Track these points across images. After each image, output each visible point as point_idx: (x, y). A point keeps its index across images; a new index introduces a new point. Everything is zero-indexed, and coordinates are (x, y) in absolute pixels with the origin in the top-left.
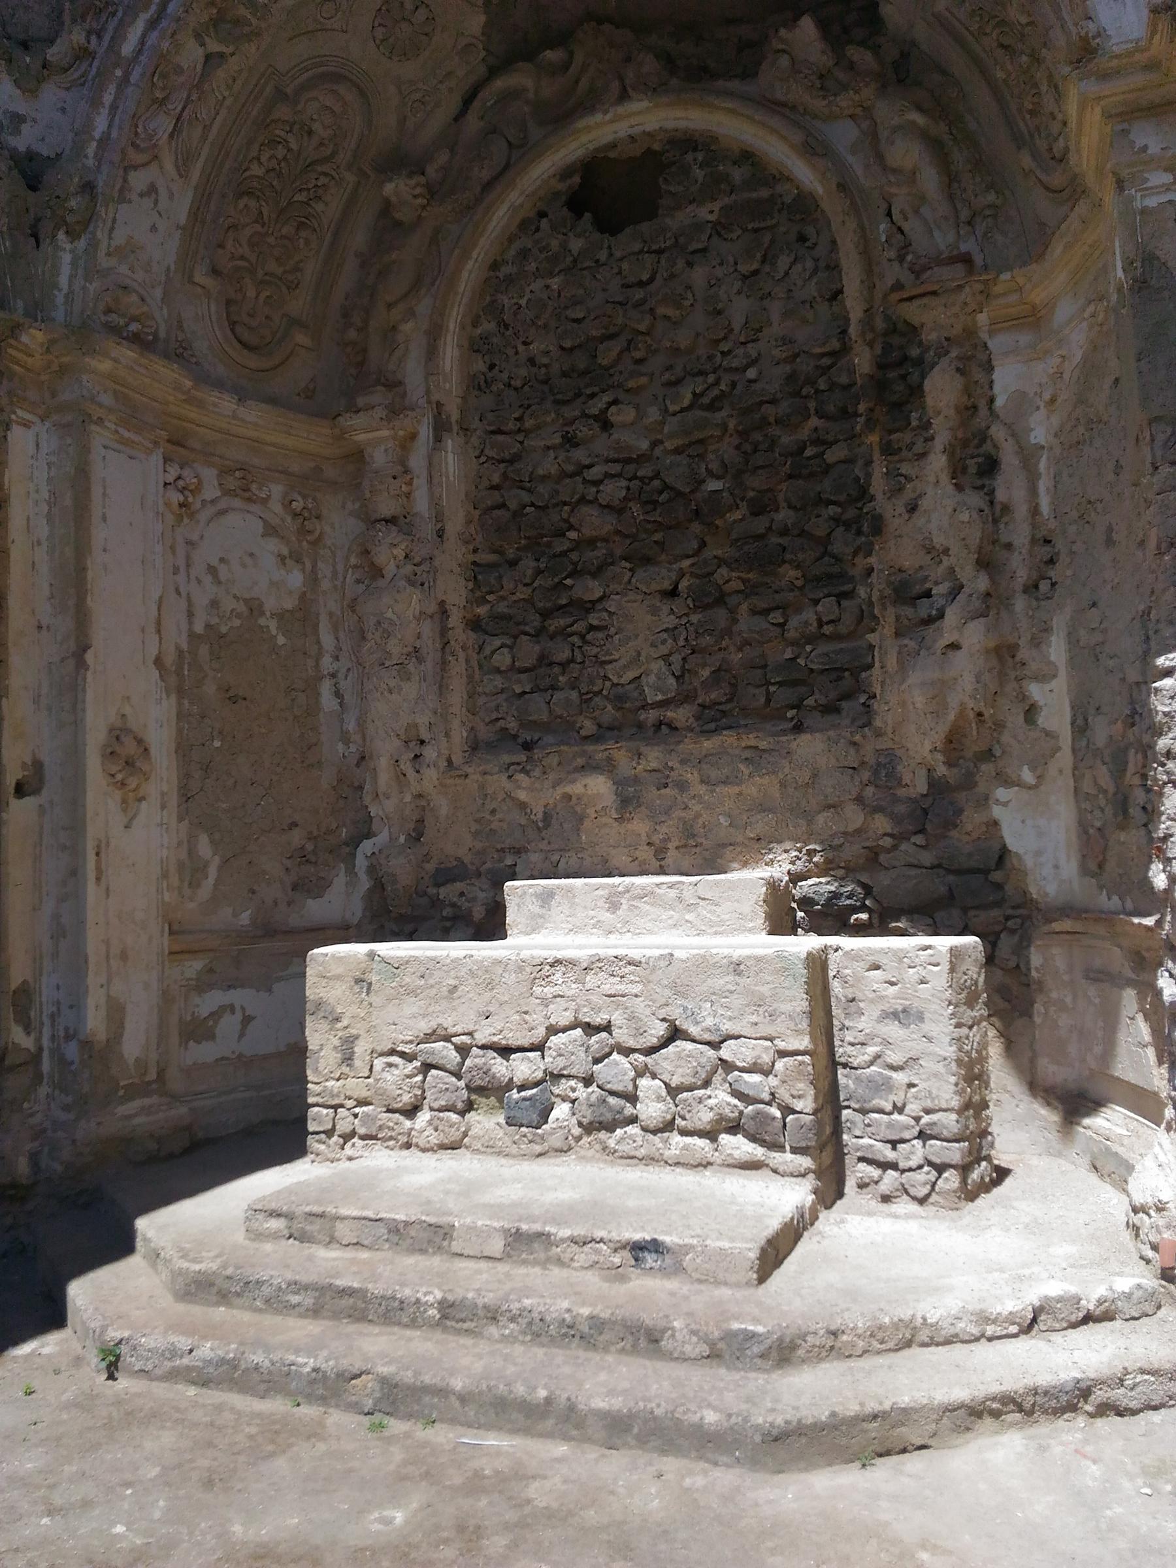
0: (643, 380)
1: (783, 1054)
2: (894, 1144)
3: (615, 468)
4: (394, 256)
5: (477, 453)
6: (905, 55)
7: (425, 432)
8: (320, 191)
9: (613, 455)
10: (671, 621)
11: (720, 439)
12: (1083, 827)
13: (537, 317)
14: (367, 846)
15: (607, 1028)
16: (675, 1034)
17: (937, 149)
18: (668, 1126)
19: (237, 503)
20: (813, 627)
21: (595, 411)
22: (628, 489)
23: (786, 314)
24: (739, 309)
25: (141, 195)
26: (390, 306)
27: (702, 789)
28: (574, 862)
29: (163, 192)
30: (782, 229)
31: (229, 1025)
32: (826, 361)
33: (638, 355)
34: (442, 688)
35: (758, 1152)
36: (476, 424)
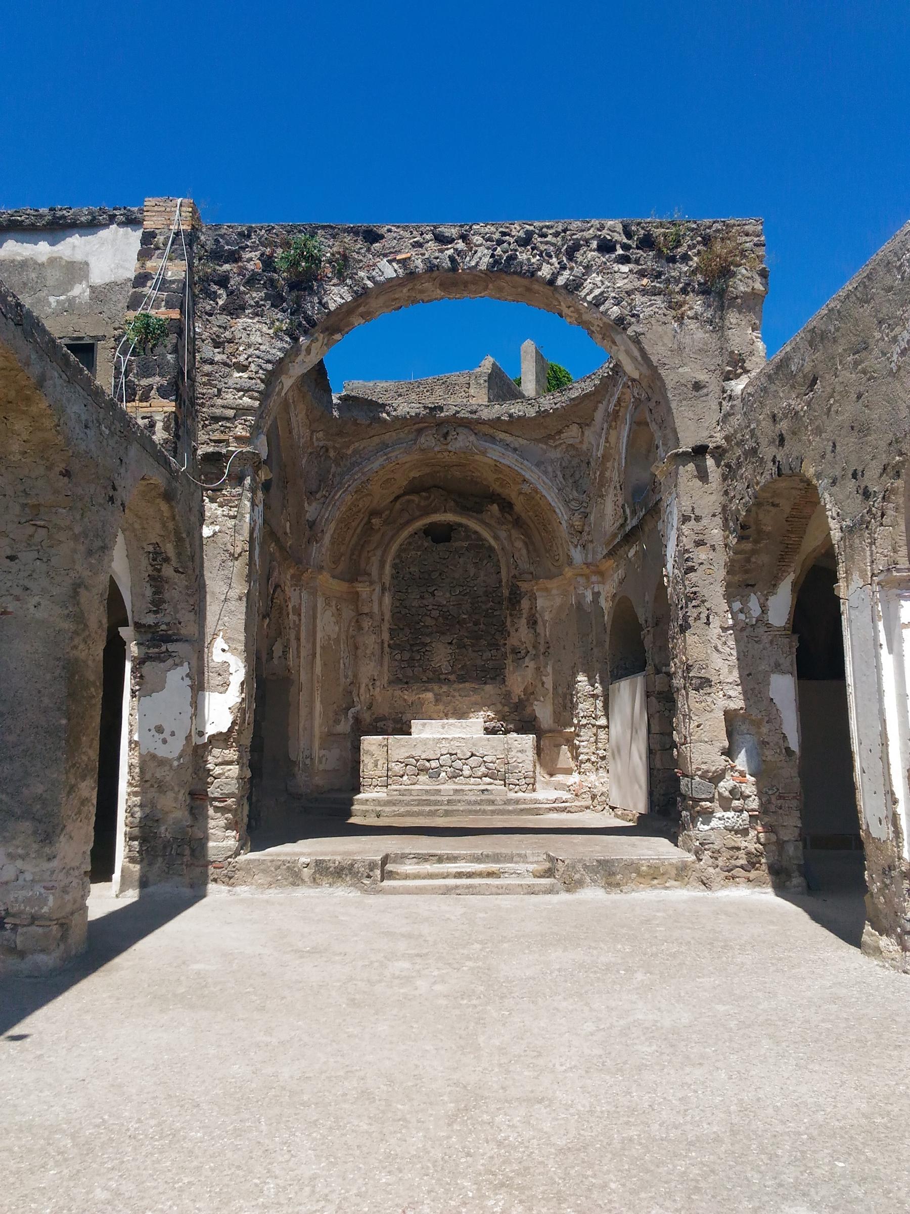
3: (436, 607)
7: (378, 588)
10: (451, 651)
12: (554, 712)
14: (353, 710)
15: (456, 754)
16: (473, 755)
17: (526, 544)
18: (470, 776)
20: (490, 657)
23: (486, 575)
24: (472, 571)
26: (368, 552)
27: (459, 698)
28: (421, 717)
31: (324, 759)
34: (382, 665)
35: (492, 781)
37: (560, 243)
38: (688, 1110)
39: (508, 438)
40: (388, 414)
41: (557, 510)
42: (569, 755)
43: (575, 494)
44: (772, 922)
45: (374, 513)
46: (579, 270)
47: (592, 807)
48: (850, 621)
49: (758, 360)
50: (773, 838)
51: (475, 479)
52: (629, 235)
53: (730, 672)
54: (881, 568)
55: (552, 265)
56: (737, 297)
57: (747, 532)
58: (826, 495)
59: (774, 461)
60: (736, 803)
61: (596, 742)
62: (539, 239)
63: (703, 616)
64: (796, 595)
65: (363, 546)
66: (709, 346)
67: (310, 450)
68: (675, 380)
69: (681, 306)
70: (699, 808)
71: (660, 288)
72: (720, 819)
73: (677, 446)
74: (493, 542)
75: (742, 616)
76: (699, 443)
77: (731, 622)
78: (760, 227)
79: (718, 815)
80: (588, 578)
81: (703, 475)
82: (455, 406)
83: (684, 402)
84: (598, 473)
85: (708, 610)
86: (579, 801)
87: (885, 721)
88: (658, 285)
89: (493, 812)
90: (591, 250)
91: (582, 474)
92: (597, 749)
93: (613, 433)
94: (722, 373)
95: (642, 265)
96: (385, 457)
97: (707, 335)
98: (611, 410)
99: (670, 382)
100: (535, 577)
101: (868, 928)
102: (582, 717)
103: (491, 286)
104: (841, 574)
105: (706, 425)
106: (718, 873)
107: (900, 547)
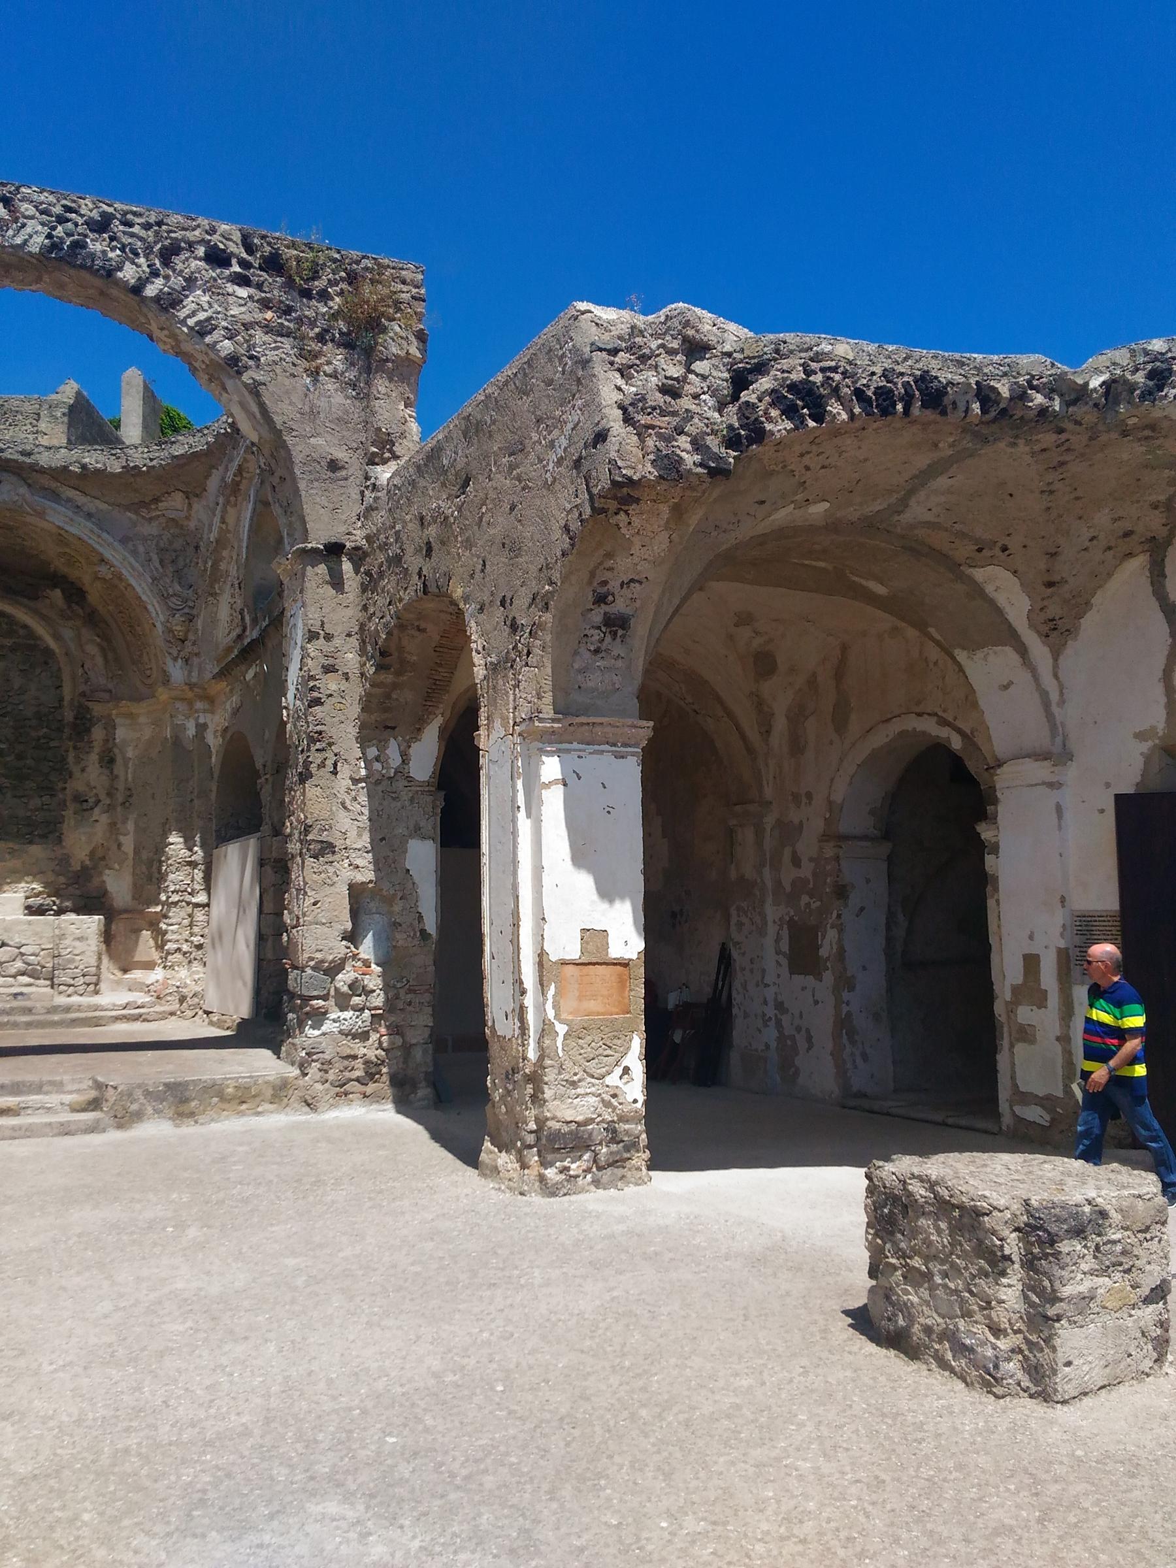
1: (43, 950)
2: (74, 978)
6: (93, 612)
12: (135, 884)
17: (102, 649)
24: (17, 682)
32: (52, 710)
35: (31, 980)
37: (151, 239)
38: (214, 1400)
39: (81, 499)
41: (150, 607)
42: (152, 943)
43: (178, 588)
44: (383, 1146)
46: (177, 282)
47: (178, 1013)
48: (489, 777)
49: (411, 445)
50: (399, 1041)
52: (250, 249)
53: (360, 835)
54: (524, 716)
55: (138, 266)
56: (387, 360)
57: (388, 660)
58: (473, 624)
59: (420, 574)
60: (356, 1000)
61: (191, 925)
62: (121, 228)
63: (329, 763)
64: (444, 743)
66: (351, 416)
68: (307, 452)
69: (316, 357)
70: (308, 1008)
71: (289, 328)
72: (334, 1021)
73: (306, 540)
75: (377, 766)
76: (333, 540)
77: (363, 772)
78: (420, 277)
79: (333, 1016)
80: (190, 704)
81: (337, 582)
83: (316, 484)
85: (336, 755)
86: (161, 1005)
87: (518, 897)
88: (286, 323)
89: (29, 1025)
90: (196, 258)
91: (188, 561)
92: (192, 934)
94: (365, 454)
95: (265, 292)
97: (348, 401)
99: (298, 457)
100: (115, 698)
101: (487, 1144)
102: (173, 892)
103: (46, 278)
104: (483, 721)
105: (344, 517)
106: (327, 1090)
107: (545, 692)
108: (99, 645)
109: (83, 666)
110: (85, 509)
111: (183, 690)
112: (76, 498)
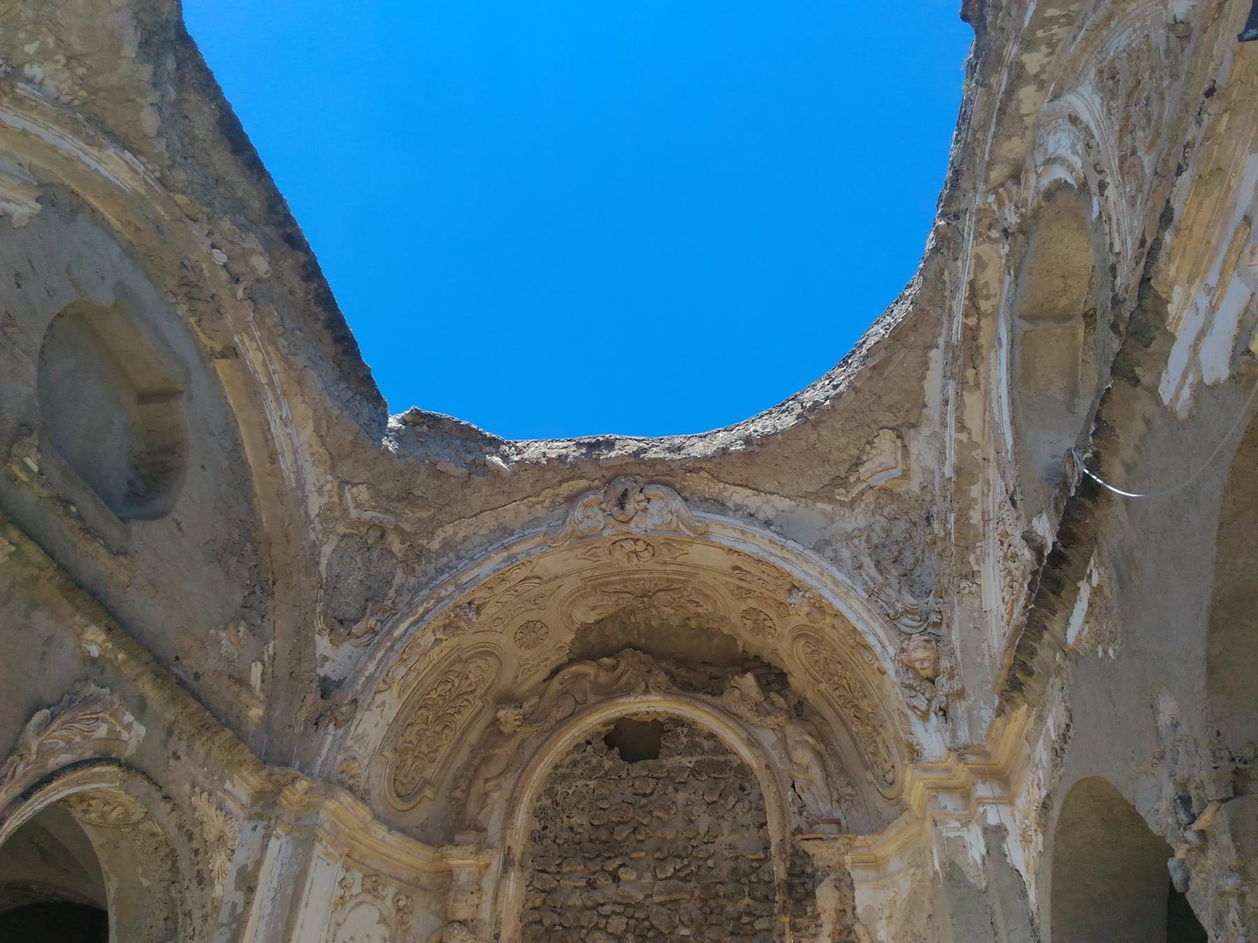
0: (643, 854)
3: (621, 909)
4: (496, 752)
5: (528, 883)
7: (496, 863)
8: (462, 709)
9: (619, 900)
11: (689, 901)
13: (579, 803)
17: (819, 755)
19: (368, 898)
21: (610, 869)
22: (627, 924)
23: (732, 831)
25: (377, 707)
26: (487, 780)
29: (387, 705)
30: (731, 781)
32: (755, 864)
33: (640, 838)
36: (529, 863)
39: (752, 500)
40: (505, 458)
41: (871, 640)
43: (909, 600)
45: (506, 699)
51: (706, 626)
65: (477, 770)
67: (341, 529)
74: (746, 754)
80: (966, 795)
82: (639, 441)
84: (952, 517)
91: (918, 552)
93: (973, 400)
96: (505, 554)
98: (957, 337)
108: (813, 749)
109: (793, 786)
110: (761, 516)
111: (947, 770)
112: (748, 501)
